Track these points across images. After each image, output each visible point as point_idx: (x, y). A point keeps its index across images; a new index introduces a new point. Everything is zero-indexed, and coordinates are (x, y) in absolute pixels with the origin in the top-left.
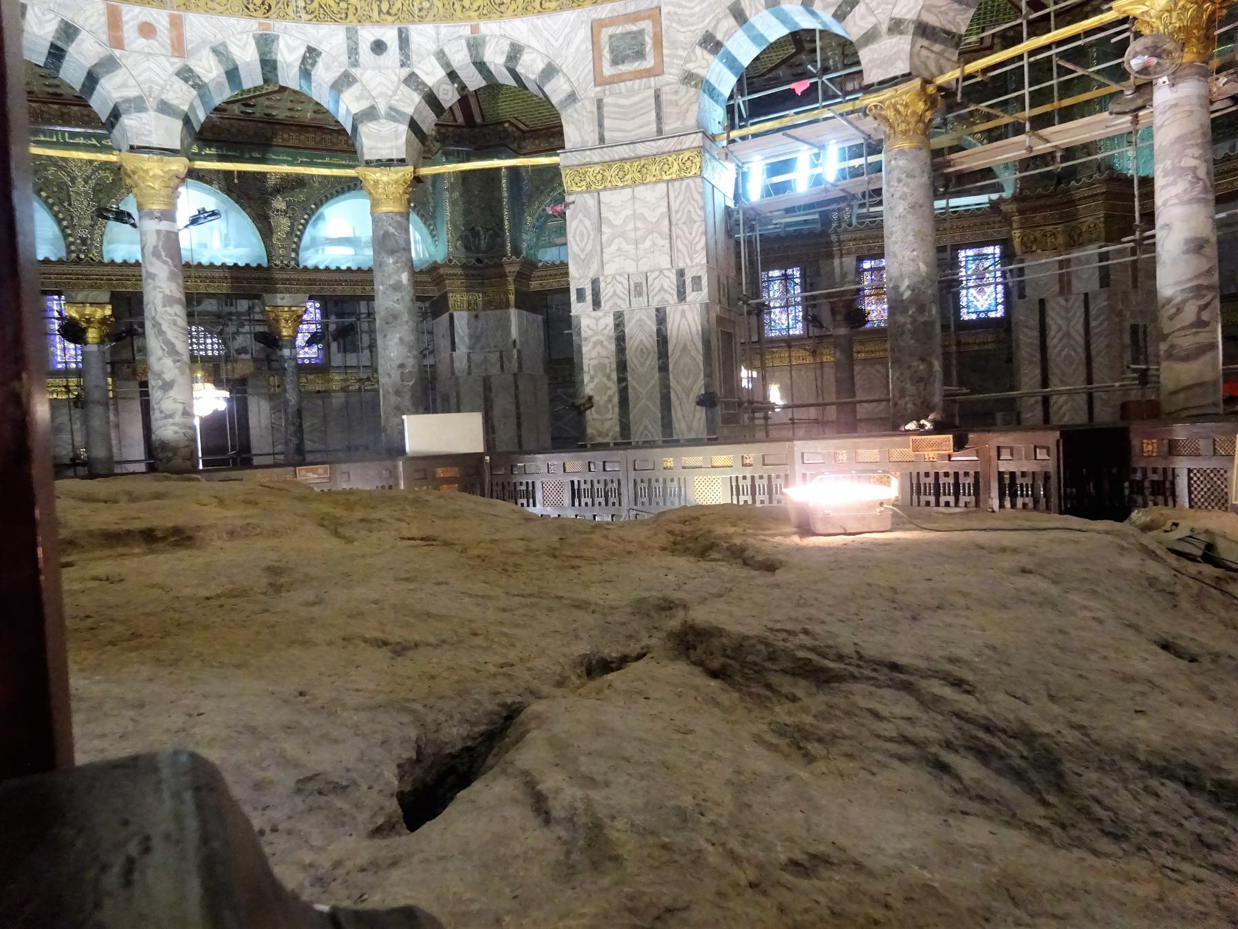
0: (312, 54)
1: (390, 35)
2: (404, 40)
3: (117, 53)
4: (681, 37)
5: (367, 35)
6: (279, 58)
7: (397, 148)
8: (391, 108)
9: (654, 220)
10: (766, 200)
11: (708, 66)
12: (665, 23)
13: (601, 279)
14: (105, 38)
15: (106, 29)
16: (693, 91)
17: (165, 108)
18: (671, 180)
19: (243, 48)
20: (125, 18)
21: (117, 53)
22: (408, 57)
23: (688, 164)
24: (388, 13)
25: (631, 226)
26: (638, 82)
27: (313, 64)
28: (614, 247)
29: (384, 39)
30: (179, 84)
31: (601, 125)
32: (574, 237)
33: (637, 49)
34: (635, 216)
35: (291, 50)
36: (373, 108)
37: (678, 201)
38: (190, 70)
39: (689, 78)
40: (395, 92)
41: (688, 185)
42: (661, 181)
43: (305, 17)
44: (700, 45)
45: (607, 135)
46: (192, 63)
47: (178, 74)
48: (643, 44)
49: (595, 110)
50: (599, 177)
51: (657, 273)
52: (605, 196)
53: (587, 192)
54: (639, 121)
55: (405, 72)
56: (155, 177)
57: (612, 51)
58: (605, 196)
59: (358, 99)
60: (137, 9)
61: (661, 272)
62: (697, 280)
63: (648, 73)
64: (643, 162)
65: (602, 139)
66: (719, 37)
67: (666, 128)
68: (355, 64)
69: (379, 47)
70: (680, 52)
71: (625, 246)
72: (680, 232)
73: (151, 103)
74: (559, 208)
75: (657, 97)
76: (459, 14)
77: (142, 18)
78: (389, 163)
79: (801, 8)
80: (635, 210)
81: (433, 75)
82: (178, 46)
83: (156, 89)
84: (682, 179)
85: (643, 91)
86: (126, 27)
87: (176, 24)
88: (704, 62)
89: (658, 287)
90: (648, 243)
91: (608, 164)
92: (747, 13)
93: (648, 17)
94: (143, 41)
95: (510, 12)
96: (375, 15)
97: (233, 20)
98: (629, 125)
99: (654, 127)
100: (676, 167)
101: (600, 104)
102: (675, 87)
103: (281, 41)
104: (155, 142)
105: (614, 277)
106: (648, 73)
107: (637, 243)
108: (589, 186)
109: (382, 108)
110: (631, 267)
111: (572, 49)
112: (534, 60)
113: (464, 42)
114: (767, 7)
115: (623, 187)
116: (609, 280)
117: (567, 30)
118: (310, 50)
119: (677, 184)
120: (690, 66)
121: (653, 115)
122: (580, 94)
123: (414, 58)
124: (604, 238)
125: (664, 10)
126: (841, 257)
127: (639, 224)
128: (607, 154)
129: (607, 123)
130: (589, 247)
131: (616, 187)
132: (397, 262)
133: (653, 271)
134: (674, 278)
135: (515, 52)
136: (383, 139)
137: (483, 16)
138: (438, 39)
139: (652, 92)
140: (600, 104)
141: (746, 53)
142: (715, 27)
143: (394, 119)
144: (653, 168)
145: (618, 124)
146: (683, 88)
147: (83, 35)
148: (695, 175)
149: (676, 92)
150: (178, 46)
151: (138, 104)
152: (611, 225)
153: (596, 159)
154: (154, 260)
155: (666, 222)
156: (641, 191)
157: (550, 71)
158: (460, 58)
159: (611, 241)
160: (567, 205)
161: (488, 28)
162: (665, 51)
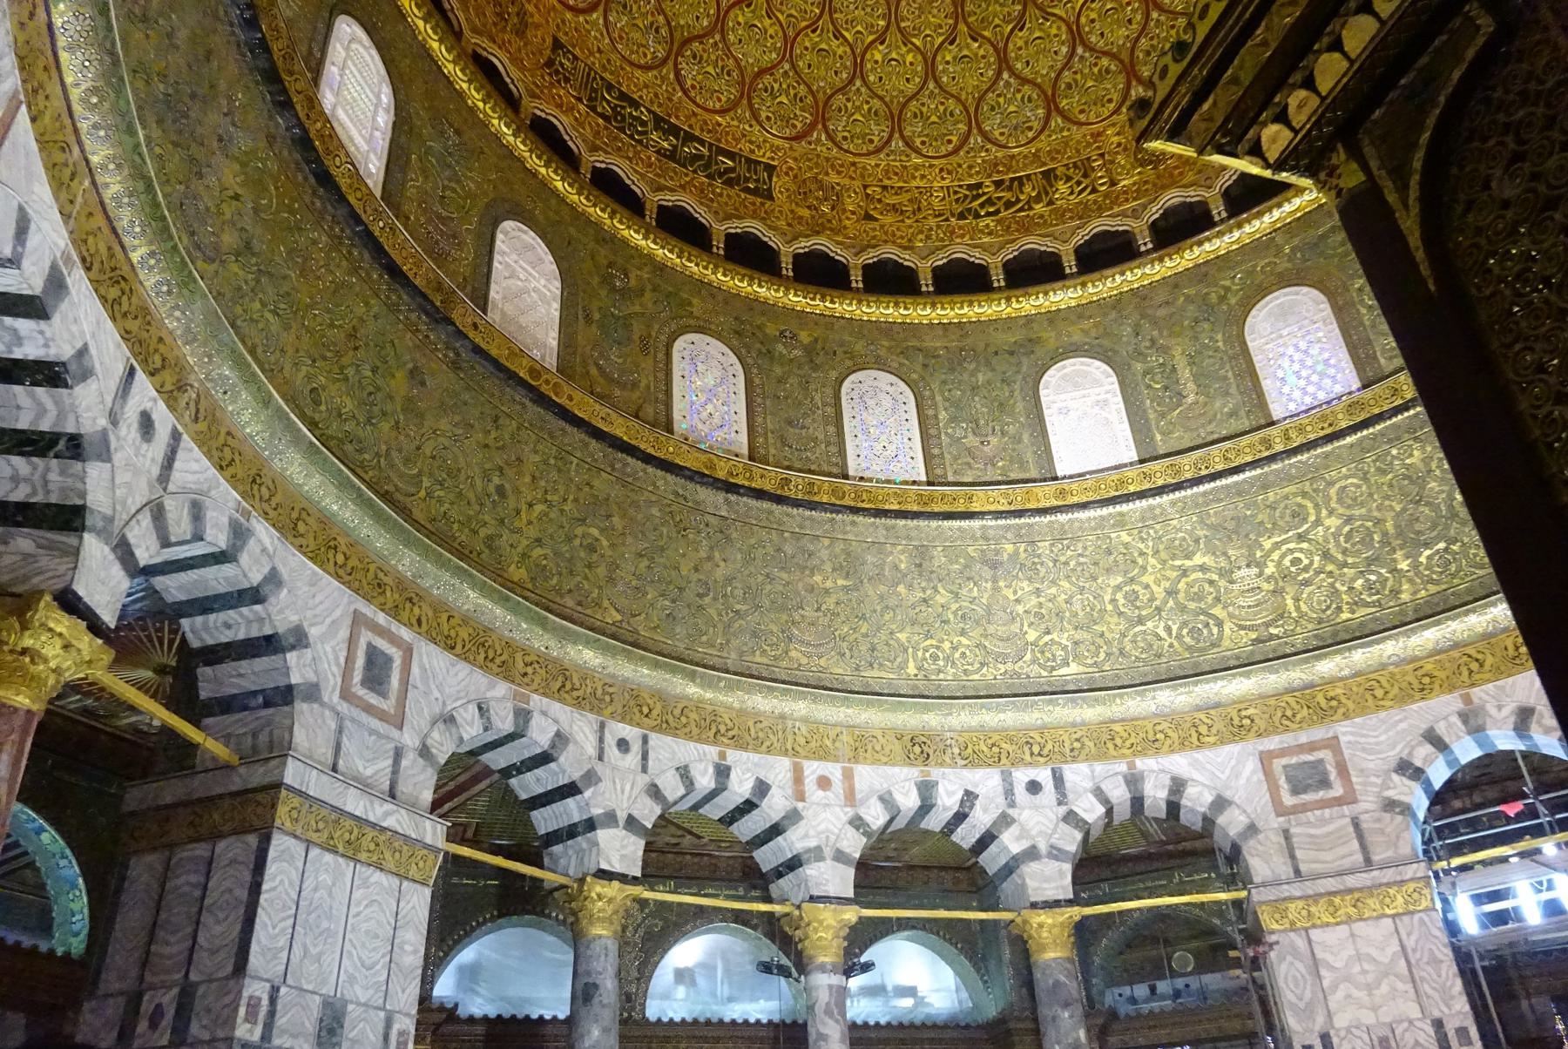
0: (970, 797)
1: (1044, 775)
2: (1058, 780)
3: (800, 805)
4: (1371, 765)
5: (1021, 776)
6: (939, 802)
7: (1063, 888)
8: (1052, 847)
9: (1386, 961)
10: (1487, 932)
11: (1412, 793)
12: (1346, 752)
13: (1332, 1033)
14: (790, 792)
15: (790, 783)
16: (1399, 818)
17: (840, 857)
18: (1398, 915)
19: (906, 794)
20: (806, 773)
21: (800, 805)
22: (1064, 795)
23: (1416, 896)
24: (1040, 755)
25: (1357, 969)
26: (1327, 811)
27: (971, 807)
28: (1340, 994)
29: (1039, 779)
30: (851, 831)
31: (1293, 857)
32: (1305, 981)
33: (1318, 778)
34: (1359, 957)
35: (950, 794)
36: (1034, 847)
37: (1413, 938)
38: (860, 818)
39: (1390, 805)
40: (1055, 831)
41: (1422, 922)
42: (1384, 916)
43: (962, 763)
44: (1396, 771)
45: (1303, 868)
46: (863, 812)
47: (851, 823)
48: (1325, 773)
49: (1282, 841)
50: (1304, 913)
51: (1406, 1025)
52: (1315, 934)
53: (1292, 930)
54: (1341, 851)
55: (1062, 810)
56: (828, 927)
57: (1289, 779)
58: (1315, 934)
59: (1018, 839)
60: (816, 764)
61: (1411, 1022)
62: (1462, 1032)
63: (1339, 802)
64: (1357, 895)
65: (1297, 872)
66: (1418, 763)
67: (1376, 858)
68: (1012, 804)
69: (1034, 787)
70: (1373, 779)
71: (1356, 993)
72: (1424, 974)
73: (828, 852)
74: (1261, 949)
75: (1356, 824)
76: (1112, 751)
77: (820, 772)
78: (1056, 904)
79: (1512, 733)
80: (1357, 950)
81: (1092, 811)
82: (850, 797)
83: (833, 838)
84: (1412, 913)
85: (1339, 821)
86: (807, 781)
87: (848, 776)
88: (1406, 790)
89: (1412, 1042)
90: (1384, 988)
91: (1316, 897)
92: (1447, 740)
93: (1326, 747)
94: (821, 793)
95: (1166, 748)
96: (1027, 757)
97: (896, 769)
98: (1328, 856)
99: (1359, 857)
100: (1400, 900)
101: (1286, 834)
102: (1377, 815)
103: (941, 787)
104: (832, 891)
105: (1348, 1030)
106: (1339, 802)
107: (1369, 988)
108: (1292, 923)
109: (1043, 847)
110: (1369, 1018)
111: (1242, 781)
112: (1201, 793)
113: (1120, 778)
114: (1469, 733)
115: (1337, 924)
116: (1343, 1033)
117: (1233, 762)
118: (968, 793)
119: (1406, 919)
120: (1391, 793)
121: (1355, 844)
122: (1260, 825)
123: (1071, 796)
124: (1326, 983)
125: (1343, 739)
126: (1528, 996)
127: (1367, 966)
128: (1310, 888)
129: (1299, 854)
130: (1308, 995)
131: (1328, 925)
132: (1071, 1017)
133: (1401, 1022)
134: (1431, 1031)
135: (1178, 786)
136: (1047, 880)
137: (1143, 753)
138: (1093, 777)
139: (1348, 820)
140: (1286, 834)
141: (1439, 774)
142: (1410, 753)
143: (1056, 858)
144: (1370, 901)
145: (1313, 854)
146: (1387, 816)
147: (773, 791)
148: (1426, 910)
149: (1379, 820)
150: (850, 797)
151: (817, 854)
152: (1332, 968)
153: (1298, 893)
154: (827, 1020)
155: (1403, 963)
156: (1359, 927)
157: (1221, 803)
158: (1119, 793)
159: (1335, 987)
160: (1271, 945)
161: (1143, 764)
162: (1354, 779)
